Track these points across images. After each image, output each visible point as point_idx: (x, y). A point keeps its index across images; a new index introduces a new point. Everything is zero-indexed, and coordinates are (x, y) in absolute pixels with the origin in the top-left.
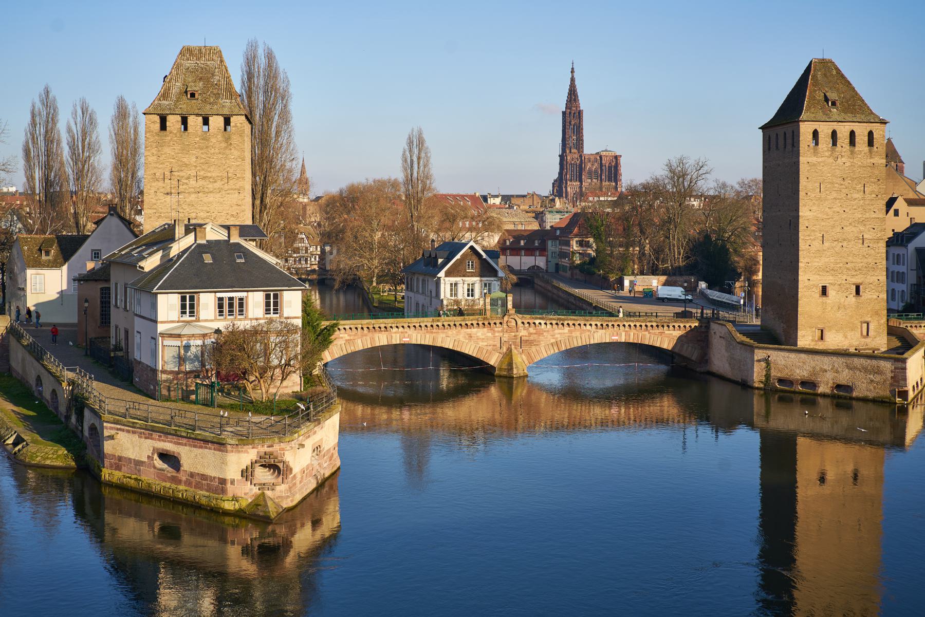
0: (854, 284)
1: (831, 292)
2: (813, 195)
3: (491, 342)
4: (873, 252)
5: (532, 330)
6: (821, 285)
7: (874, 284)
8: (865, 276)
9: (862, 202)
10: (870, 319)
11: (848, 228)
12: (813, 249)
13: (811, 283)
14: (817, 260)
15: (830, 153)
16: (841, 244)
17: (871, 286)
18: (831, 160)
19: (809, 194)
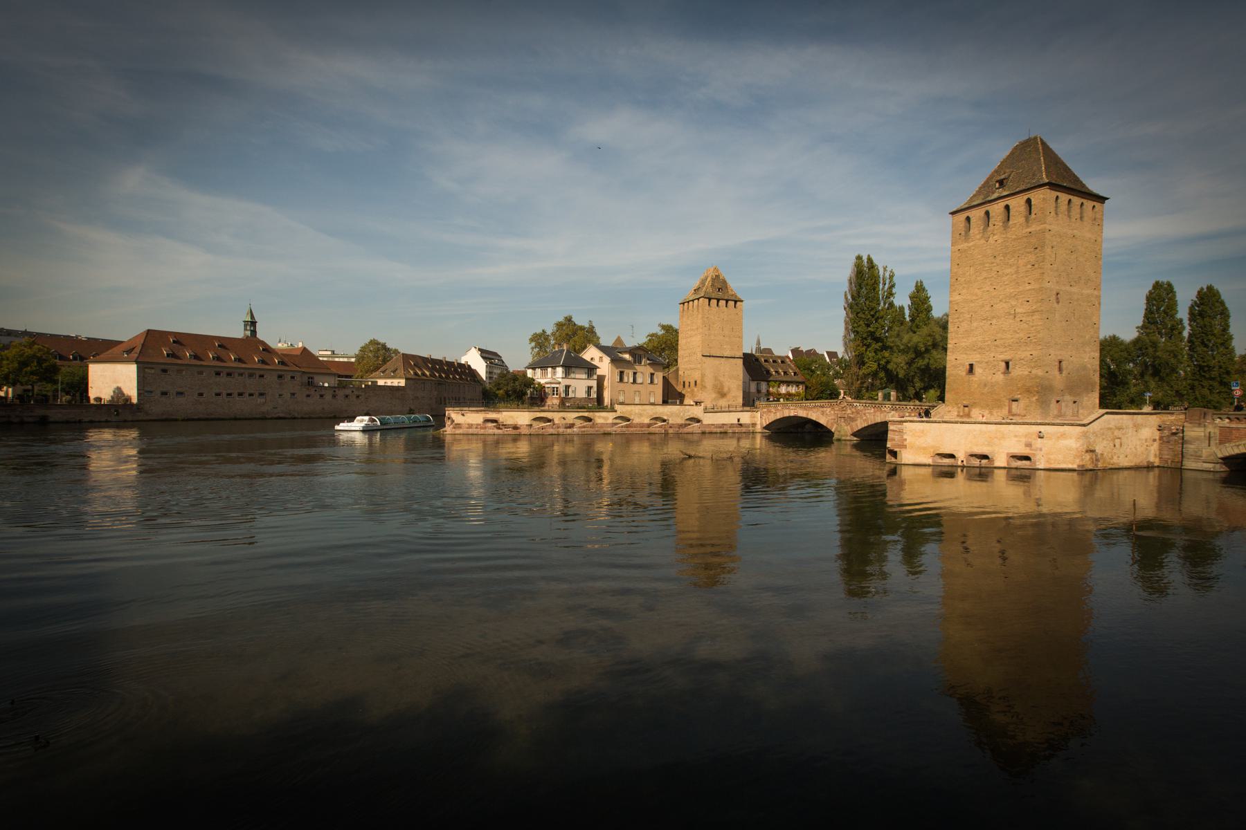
0: (1002, 361)
1: (977, 370)
2: (964, 279)
3: (833, 417)
4: (1027, 326)
5: (853, 410)
6: (967, 364)
7: (1026, 359)
8: (1015, 352)
9: (1014, 276)
10: (1019, 396)
11: (999, 305)
12: (961, 330)
13: (958, 362)
14: (965, 340)
15: (981, 235)
16: (989, 322)
17: (1022, 361)
18: (983, 241)
19: (959, 279)
